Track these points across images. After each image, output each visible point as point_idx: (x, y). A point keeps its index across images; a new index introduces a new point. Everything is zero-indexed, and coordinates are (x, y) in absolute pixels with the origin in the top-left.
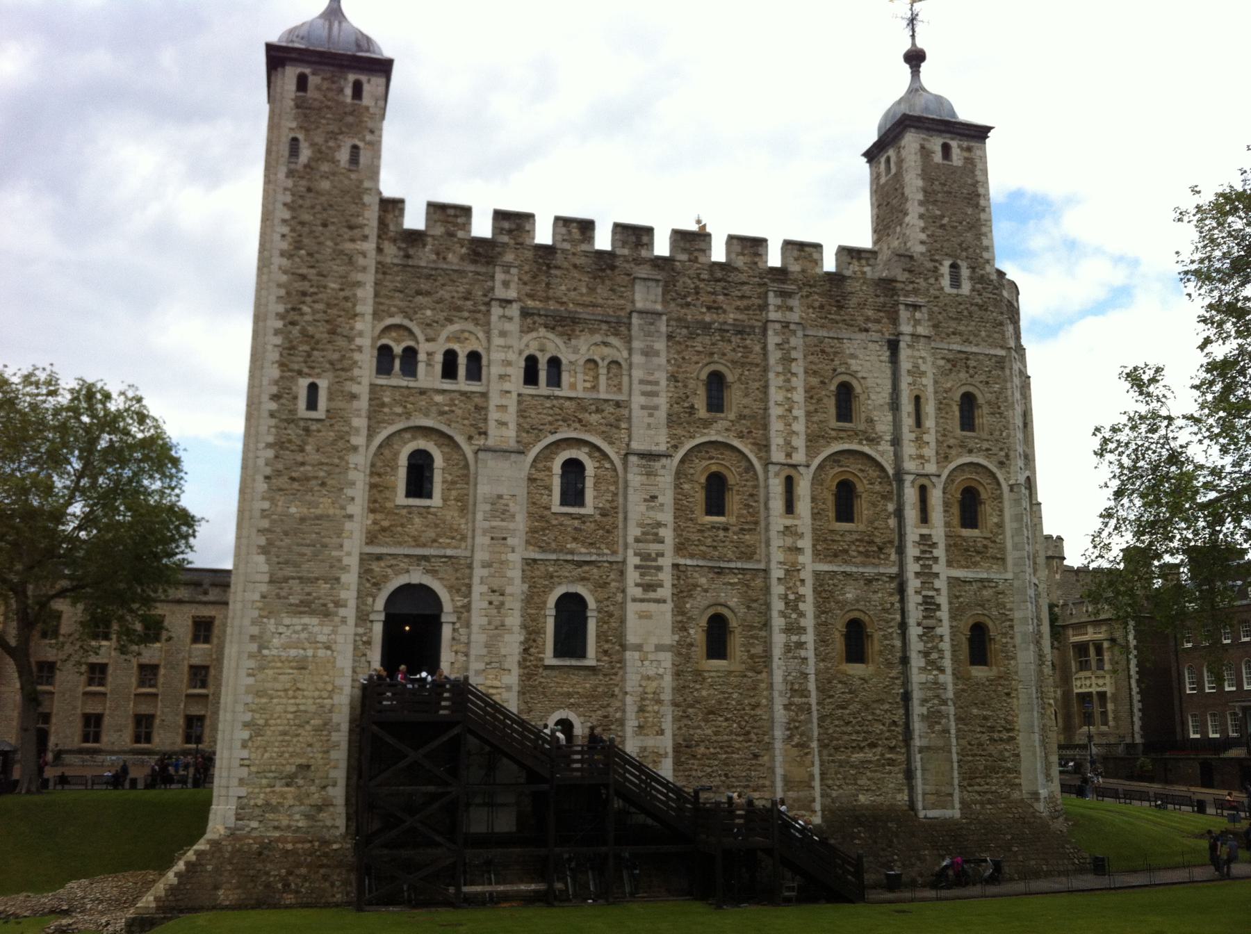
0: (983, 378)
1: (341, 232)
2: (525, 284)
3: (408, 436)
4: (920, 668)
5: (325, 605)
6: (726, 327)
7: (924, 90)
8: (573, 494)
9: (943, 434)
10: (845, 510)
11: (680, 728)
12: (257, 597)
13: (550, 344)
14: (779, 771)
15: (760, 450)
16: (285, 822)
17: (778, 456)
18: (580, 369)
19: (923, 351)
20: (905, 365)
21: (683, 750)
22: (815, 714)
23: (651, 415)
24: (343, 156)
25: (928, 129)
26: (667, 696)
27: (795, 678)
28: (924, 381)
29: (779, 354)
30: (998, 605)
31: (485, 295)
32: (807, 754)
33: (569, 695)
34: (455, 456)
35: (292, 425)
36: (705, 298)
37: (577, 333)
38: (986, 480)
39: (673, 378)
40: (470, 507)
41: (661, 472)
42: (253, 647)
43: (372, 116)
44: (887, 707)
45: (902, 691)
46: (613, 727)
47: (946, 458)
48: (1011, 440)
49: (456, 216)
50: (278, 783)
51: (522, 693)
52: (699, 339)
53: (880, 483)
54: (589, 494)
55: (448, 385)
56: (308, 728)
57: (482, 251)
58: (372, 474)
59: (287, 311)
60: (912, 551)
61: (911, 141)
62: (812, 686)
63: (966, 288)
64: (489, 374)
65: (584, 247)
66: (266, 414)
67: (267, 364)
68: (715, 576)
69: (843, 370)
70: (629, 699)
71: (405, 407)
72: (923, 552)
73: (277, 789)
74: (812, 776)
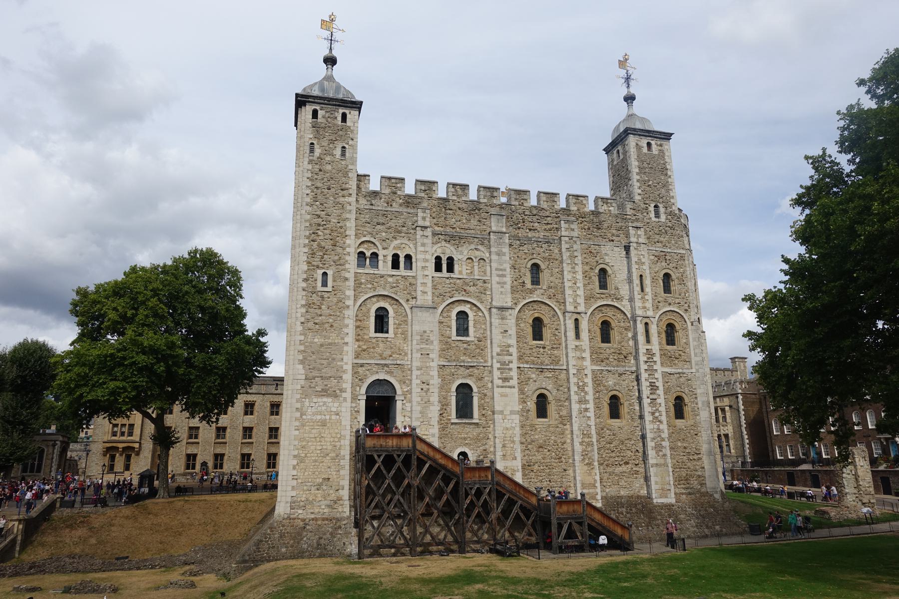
0: (674, 265)
1: (337, 192)
2: (434, 218)
3: (374, 299)
4: (650, 421)
5: (335, 391)
6: (540, 240)
8: (463, 330)
10: (606, 337)
11: (524, 456)
12: (299, 387)
14: (578, 478)
15: (560, 305)
16: (317, 511)
17: (570, 308)
18: (464, 263)
19: (644, 250)
20: (634, 259)
21: (527, 467)
22: (596, 447)
23: (502, 287)
24: (338, 152)
25: (640, 135)
26: (517, 439)
27: (585, 427)
28: (644, 267)
29: (568, 254)
30: (688, 386)
31: (413, 225)
32: (592, 469)
33: (465, 439)
34: (400, 310)
35: (314, 295)
36: (527, 224)
37: (462, 244)
39: (513, 267)
40: (410, 338)
41: (509, 317)
42: (298, 414)
43: (352, 131)
44: (633, 442)
45: (640, 433)
46: (489, 456)
47: (657, 308)
48: (691, 298)
49: (397, 183)
50: (313, 488)
51: (440, 438)
52: (526, 246)
53: (624, 322)
54: (471, 330)
55: (395, 272)
56: (328, 458)
57: (410, 201)
58: (357, 320)
59: (310, 234)
60: (643, 358)
61: (632, 140)
62: (593, 432)
63: (663, 218)
65: (464, 198)
66: (300, 289)
68: (540, 373)
69: (602, 262)
70: (497, 440)
71: (373, 285)
72: (648, 358)
73: (312, 492)
74: (595, 481)
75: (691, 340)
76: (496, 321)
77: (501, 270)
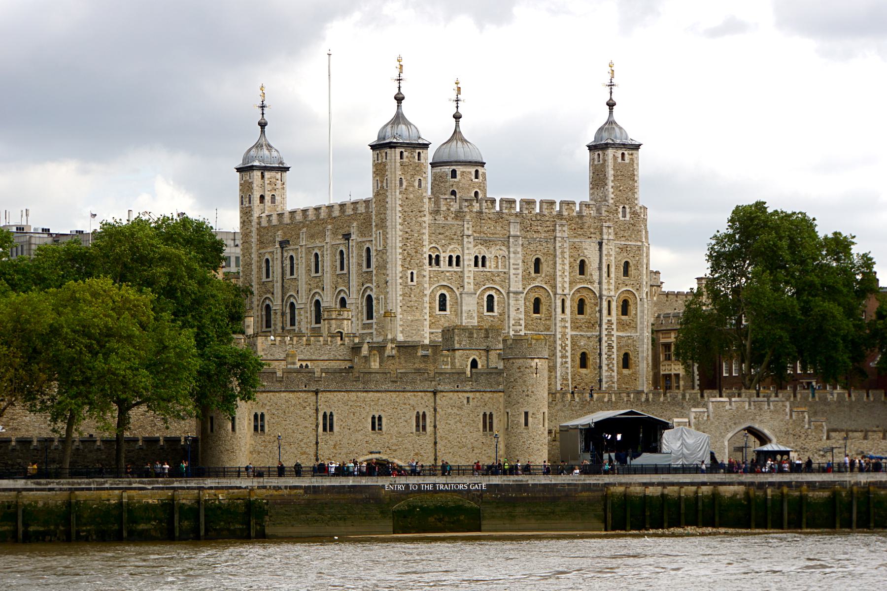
7: (615, 123)
8: (490, 308)
9: (617, 278)
10: (581, 311)
13: (482, 251)
17: (559, 291)
20: (604, 252)
24: (416, 184)
28: (611, 258)
36: (534, 228)
38: (631, 296)
40: (459, 315)
55: (450, 269)
60: (604, 326)
61: (610, 152)
62: (570, 377)
64: (464, 264)
65: (493, 211)
66: (398, 284)
67: (398, 266)
75: (638, 311)
76: (512, 302)
77: (516, 264)
